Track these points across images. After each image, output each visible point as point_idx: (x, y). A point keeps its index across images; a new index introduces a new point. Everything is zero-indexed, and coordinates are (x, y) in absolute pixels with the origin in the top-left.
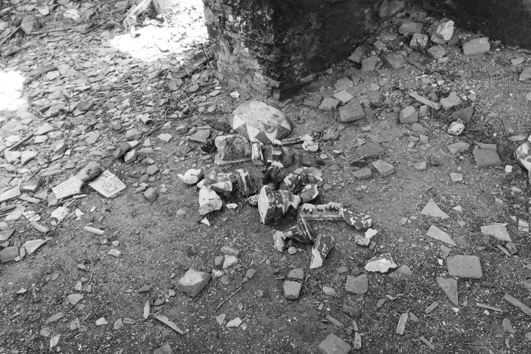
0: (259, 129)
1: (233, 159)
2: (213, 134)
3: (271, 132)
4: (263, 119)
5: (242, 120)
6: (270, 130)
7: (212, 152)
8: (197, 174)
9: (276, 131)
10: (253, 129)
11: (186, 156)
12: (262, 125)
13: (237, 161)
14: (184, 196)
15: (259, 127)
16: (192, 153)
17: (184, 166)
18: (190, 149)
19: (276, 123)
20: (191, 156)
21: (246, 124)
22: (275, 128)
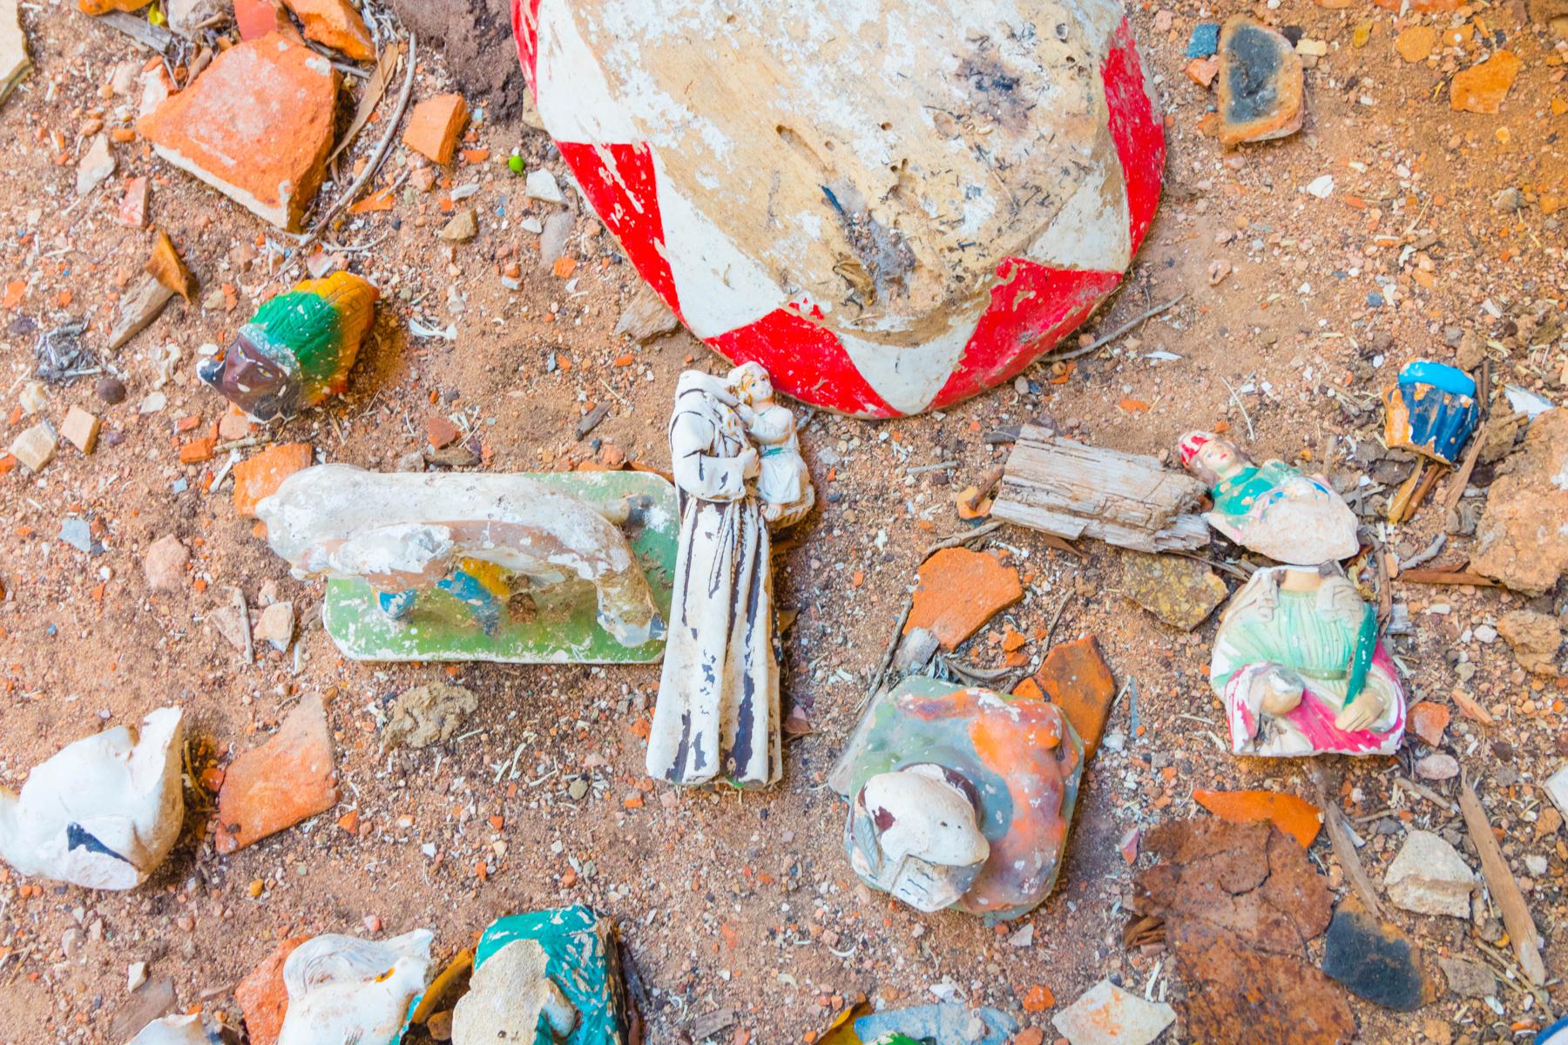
0: (784, 279)
1: (490, 628)
2: (369, 94)
3: (909, 340)
4: (838, 113)
5: (616, 82)
6: (891, 321)
7: (330, 403)
8: (117, 839)
9: (963, 329)
10: (724, 250)
11: (117, 394)
12: (816, 224)
13: (529, 658)
14: (42, 1005)
15: (778, 251)
16: (155, 356)
17: (77, 532)
18: (149, 290)
19: (979, 215)
20: (155, 402)
21: (647, 162)
22: (952, 303)
